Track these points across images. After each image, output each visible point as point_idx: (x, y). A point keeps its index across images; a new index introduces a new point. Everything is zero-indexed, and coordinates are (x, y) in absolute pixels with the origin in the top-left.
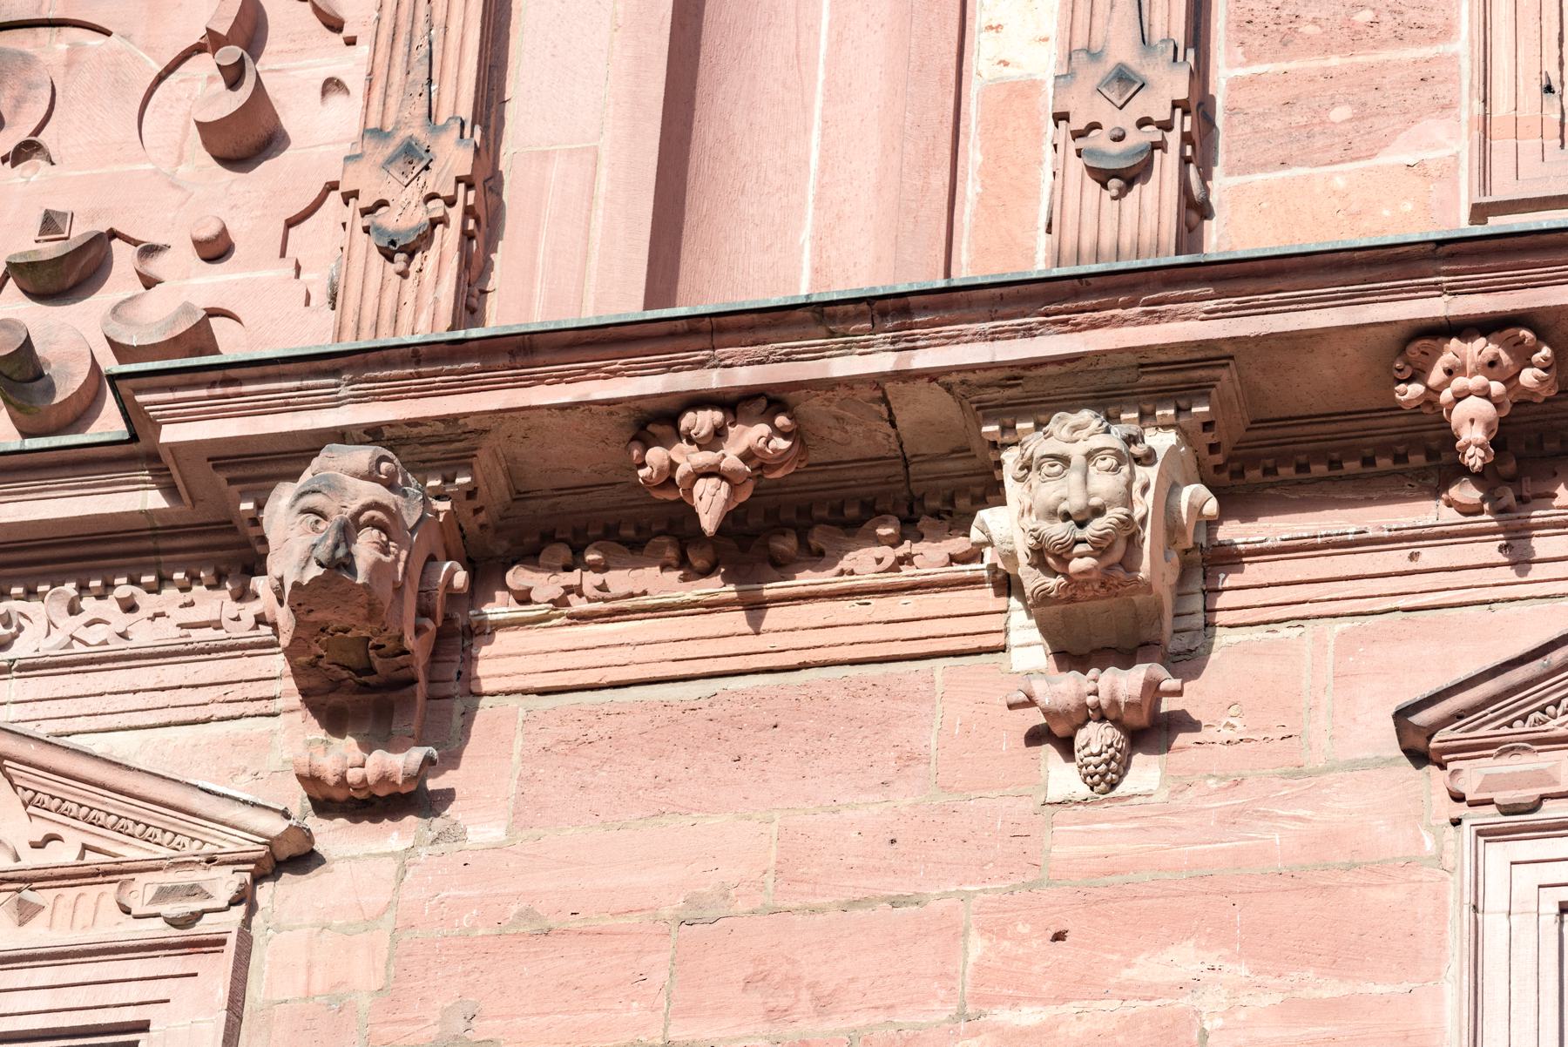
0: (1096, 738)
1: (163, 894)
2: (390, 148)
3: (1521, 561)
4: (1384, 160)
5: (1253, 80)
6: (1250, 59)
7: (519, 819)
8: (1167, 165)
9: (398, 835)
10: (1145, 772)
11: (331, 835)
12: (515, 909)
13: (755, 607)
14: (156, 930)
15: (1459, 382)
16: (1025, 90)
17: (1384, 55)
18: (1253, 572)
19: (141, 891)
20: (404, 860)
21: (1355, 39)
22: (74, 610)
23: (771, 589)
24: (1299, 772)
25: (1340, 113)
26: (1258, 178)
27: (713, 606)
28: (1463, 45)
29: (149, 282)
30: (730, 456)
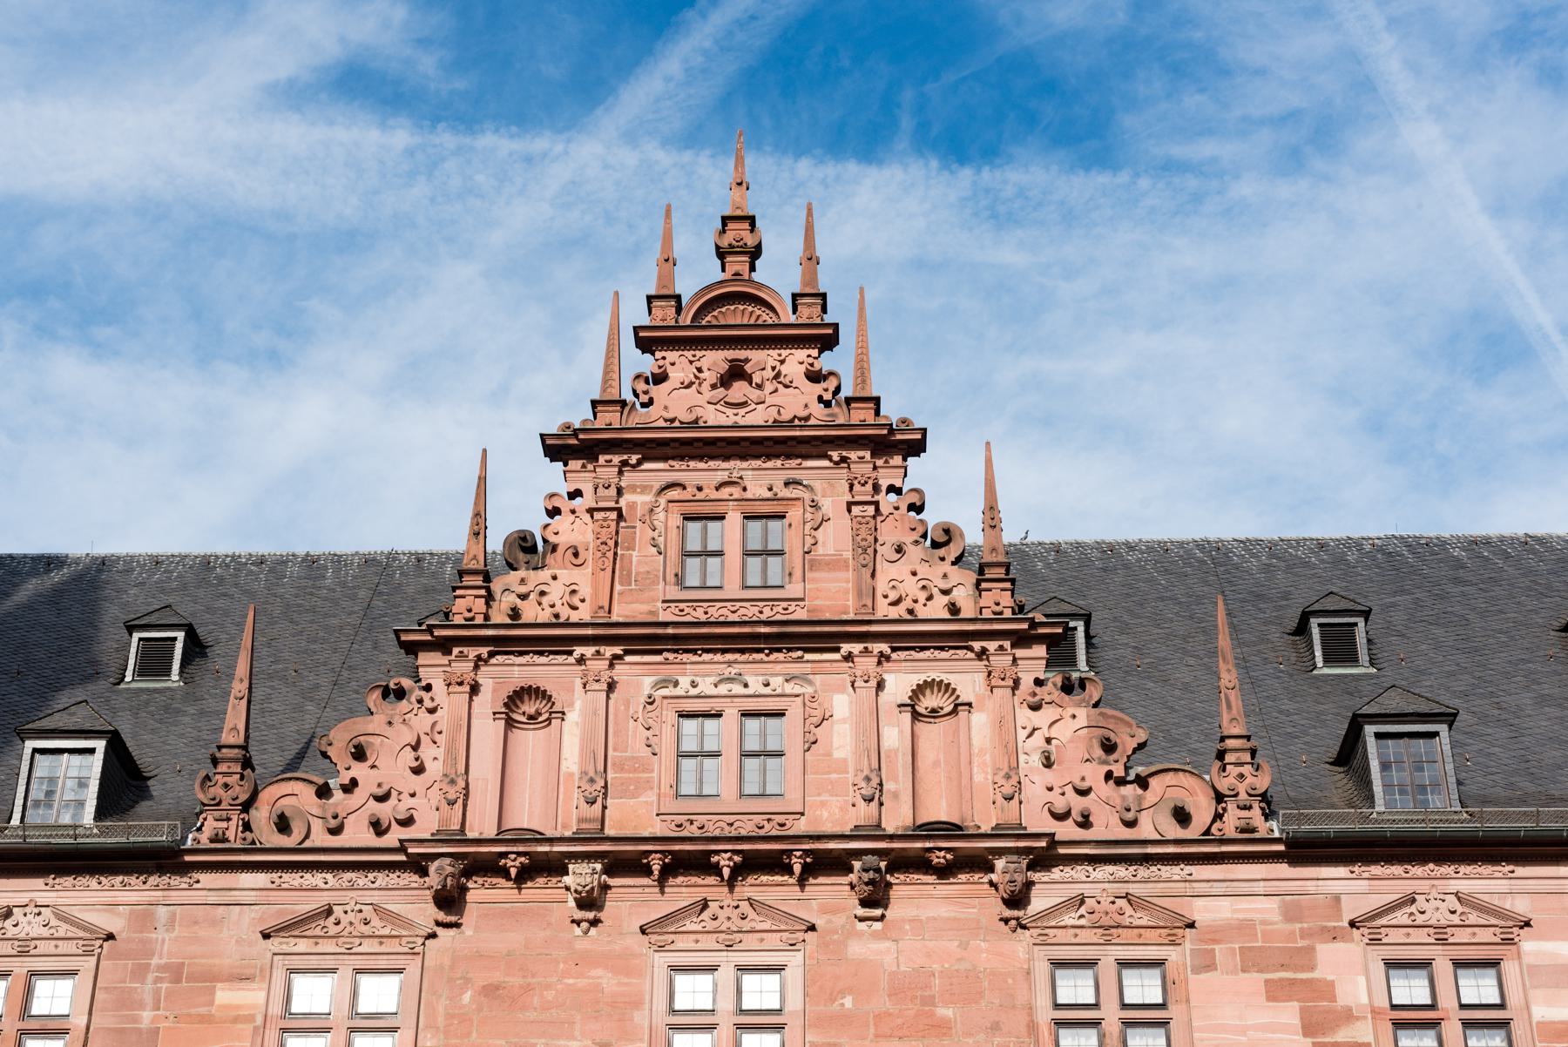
0: (585, 925)
1: (408, 943)
2: (448, 780)
3: (662, 892)
4: (640, 799)
5: (616, 777)
6: (616, 772)
7: (477, 929)
8: (600, 800)
9: (452, 932)
10: (593, 931)
11: (440, 931)
12: (475, 950)
13: (520, 889)
14: (406, 950)
15: (654, 861)
16: (571, 775)
17: (641, 775)
18: (614, 890)
19: (404, 941)
20: (453, 937)
21: (635, 771)
22: (388, 876)
23: (523, 886)
24: (621, 934)
25: (632, 787)
26: (616, 801)
27: (512, 888)
28: (655, 775)
29: (399, 801)
30: (517, 863)
